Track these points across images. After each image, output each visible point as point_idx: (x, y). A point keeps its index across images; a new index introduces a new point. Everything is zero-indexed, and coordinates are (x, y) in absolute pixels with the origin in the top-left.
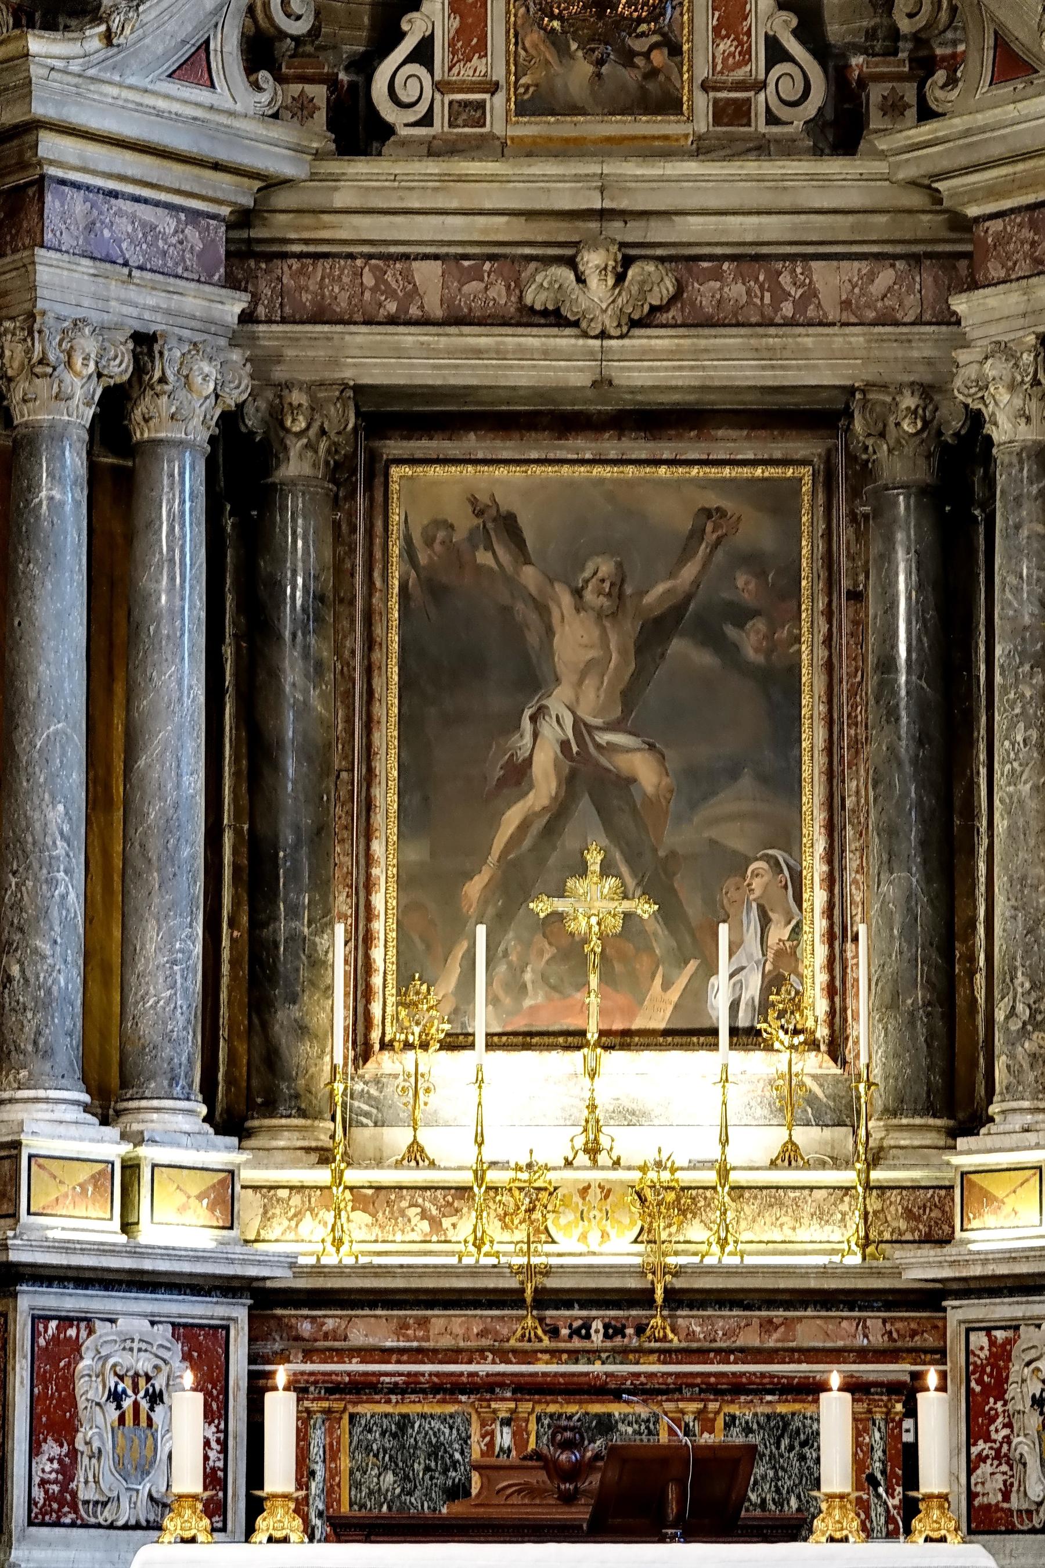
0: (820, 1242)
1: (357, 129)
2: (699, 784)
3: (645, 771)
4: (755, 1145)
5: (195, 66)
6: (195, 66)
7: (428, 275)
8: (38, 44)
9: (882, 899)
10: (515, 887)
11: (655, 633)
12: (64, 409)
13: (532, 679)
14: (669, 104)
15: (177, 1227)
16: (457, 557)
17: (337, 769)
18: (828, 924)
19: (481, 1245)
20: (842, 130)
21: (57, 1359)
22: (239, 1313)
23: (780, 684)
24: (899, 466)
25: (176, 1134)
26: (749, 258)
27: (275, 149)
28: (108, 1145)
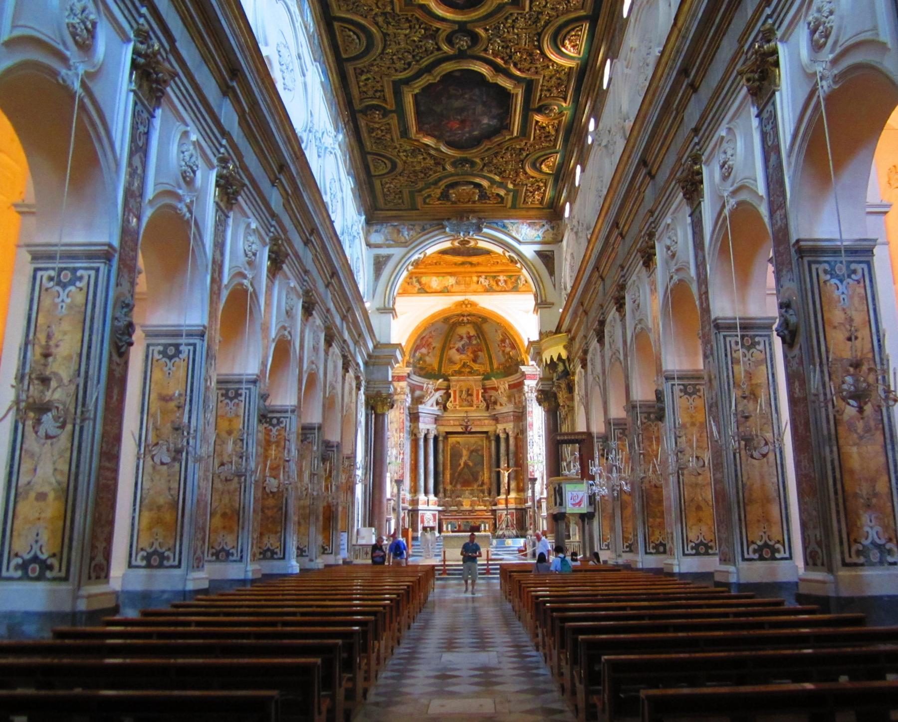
1: (445, 408)
3: (471, 464)
5: (432, 406)
6: (432, 406)
7: (452, 422)
8: (420, 406)
12: (422, 436)
13: (461, 456)
14: (472, 406)
16: (454, 446)
21: (422, 517)
22: (437, 513)
23: (483, 456)
24: (492, 438)
26: (479, 420)
28: (426, 498)
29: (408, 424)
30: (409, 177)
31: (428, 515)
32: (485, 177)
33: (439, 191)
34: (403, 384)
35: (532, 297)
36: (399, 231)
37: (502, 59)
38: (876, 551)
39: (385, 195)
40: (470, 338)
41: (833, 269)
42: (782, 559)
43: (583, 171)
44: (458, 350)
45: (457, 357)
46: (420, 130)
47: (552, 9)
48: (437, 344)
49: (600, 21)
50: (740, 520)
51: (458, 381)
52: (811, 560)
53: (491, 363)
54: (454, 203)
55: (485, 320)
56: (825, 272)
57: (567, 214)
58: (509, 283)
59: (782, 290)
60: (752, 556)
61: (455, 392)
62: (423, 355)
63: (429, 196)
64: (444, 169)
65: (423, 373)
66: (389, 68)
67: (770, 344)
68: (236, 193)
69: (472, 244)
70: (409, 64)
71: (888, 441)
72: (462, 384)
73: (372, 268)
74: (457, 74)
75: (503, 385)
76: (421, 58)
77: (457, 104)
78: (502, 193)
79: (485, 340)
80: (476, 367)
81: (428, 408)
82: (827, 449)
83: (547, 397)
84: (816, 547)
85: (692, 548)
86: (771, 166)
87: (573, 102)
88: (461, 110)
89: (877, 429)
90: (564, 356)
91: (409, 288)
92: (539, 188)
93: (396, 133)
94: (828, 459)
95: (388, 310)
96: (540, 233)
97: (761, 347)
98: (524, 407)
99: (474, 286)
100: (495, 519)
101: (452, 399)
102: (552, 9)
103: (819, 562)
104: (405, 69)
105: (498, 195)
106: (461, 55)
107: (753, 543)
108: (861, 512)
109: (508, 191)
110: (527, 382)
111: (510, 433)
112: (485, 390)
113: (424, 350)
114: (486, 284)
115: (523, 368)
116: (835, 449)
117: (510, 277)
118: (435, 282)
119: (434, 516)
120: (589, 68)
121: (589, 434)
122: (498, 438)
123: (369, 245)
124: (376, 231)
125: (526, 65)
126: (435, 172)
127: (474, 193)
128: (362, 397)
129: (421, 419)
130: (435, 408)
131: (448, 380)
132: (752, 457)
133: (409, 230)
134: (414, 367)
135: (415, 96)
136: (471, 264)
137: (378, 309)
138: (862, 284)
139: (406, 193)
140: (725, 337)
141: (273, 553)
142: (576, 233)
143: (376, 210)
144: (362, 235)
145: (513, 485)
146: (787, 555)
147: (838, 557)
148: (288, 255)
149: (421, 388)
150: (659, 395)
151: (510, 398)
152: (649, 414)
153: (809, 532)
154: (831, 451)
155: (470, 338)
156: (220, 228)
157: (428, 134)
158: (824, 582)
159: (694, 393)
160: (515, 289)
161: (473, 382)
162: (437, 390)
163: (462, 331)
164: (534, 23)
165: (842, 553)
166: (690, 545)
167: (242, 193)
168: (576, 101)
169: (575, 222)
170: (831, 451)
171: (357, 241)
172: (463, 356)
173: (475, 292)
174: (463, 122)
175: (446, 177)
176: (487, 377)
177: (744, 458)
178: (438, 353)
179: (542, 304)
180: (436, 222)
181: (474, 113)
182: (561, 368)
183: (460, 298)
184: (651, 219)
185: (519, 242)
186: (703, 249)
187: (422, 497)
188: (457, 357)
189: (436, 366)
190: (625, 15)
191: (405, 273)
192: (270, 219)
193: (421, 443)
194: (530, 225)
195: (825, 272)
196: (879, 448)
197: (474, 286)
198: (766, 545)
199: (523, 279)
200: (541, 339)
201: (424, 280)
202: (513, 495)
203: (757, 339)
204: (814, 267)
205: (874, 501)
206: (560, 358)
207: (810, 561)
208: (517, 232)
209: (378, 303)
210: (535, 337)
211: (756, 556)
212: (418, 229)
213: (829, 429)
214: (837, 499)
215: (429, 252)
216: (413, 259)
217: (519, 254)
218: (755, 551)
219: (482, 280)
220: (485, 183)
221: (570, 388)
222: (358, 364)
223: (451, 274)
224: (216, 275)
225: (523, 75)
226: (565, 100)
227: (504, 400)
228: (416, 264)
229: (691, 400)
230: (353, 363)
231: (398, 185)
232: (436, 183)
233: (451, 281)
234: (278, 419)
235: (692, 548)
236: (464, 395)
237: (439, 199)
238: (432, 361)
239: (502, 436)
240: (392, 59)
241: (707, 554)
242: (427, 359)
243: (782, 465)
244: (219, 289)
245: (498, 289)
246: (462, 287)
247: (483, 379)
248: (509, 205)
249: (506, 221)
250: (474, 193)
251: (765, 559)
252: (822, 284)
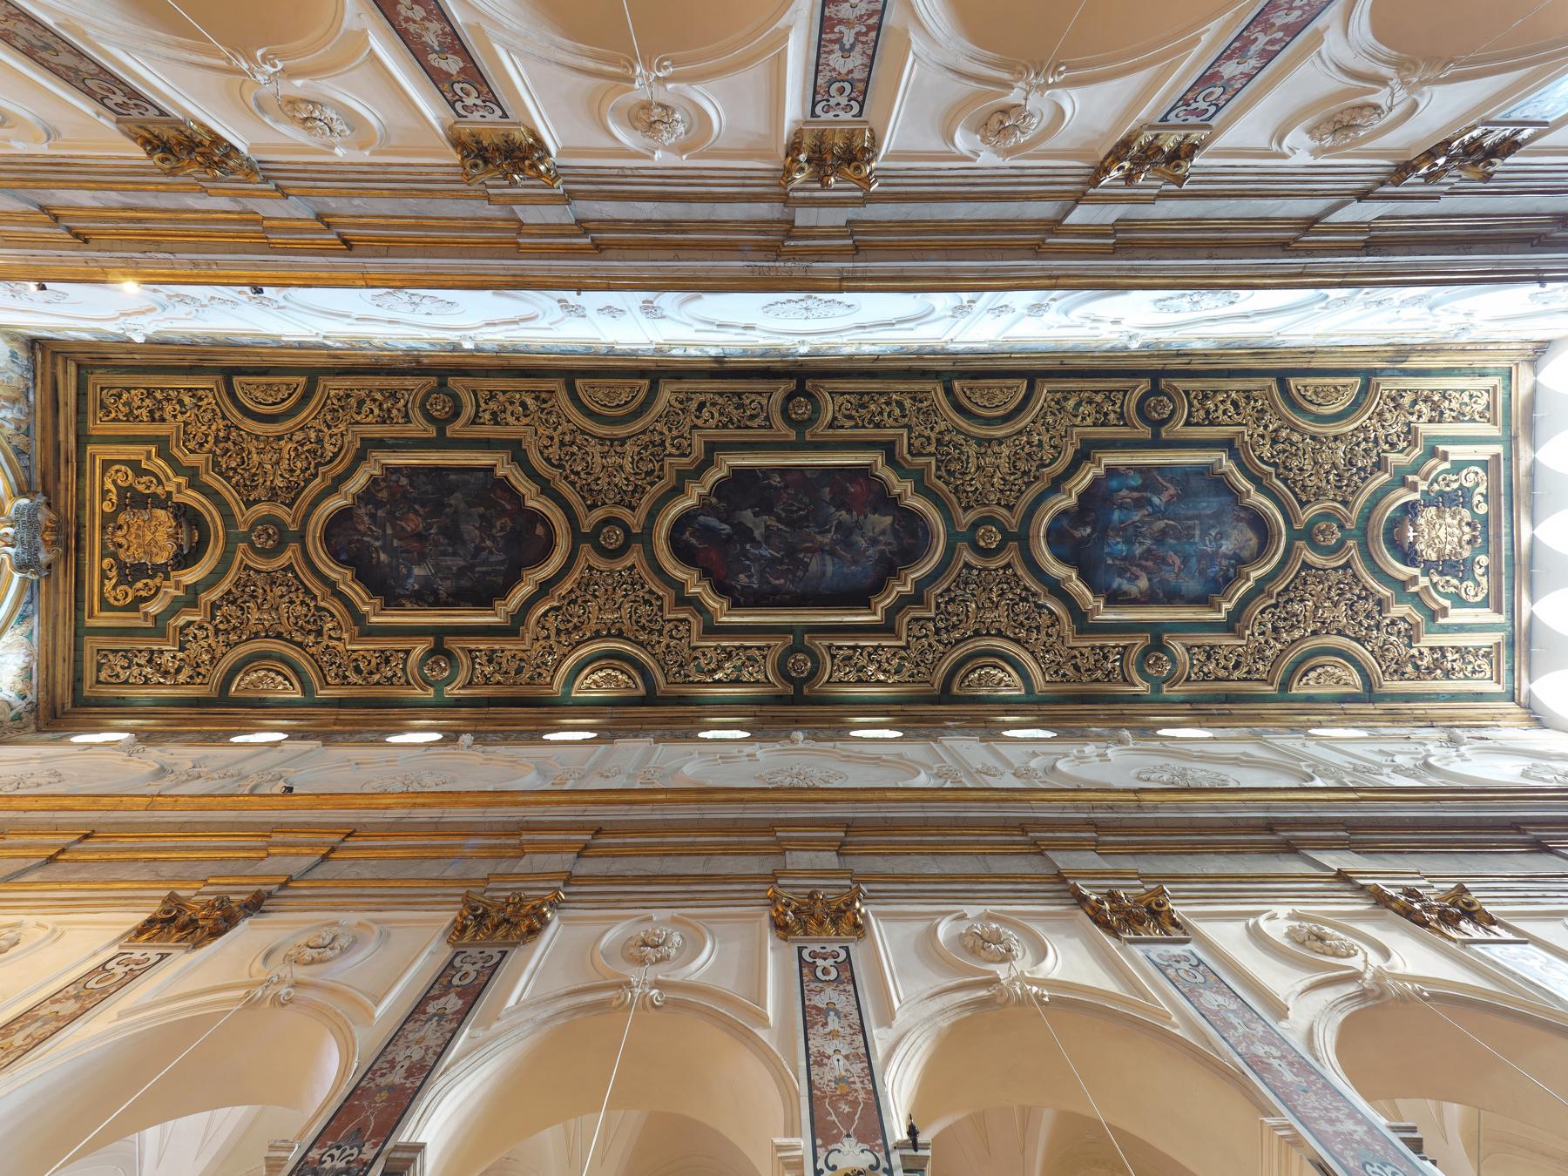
37: (572, 591)
46: (388, 469)
47: (668, 646)
49: (644, 709)
66: (552, 439)
70: (562, 467)
74: (540, 530)
76: (573, 484)
77: (470, 530)
87: (457, 700)
88: (453, 535)
93: (377, 431)
102: (668, 646)
104: (548, 460)
106: (577, 537)
120: (546, 709)
125: (552, 623)
135: (490, 470)
157: (374, 481)
164: (643, 628)
168: (459, 703)
174: (420, 537)
181: (444, 554)
190: (701, 735)
212: (19, 440)
225: (533, 620)
226: (470, 684)
240: (573, 443)
249: (36, 618)
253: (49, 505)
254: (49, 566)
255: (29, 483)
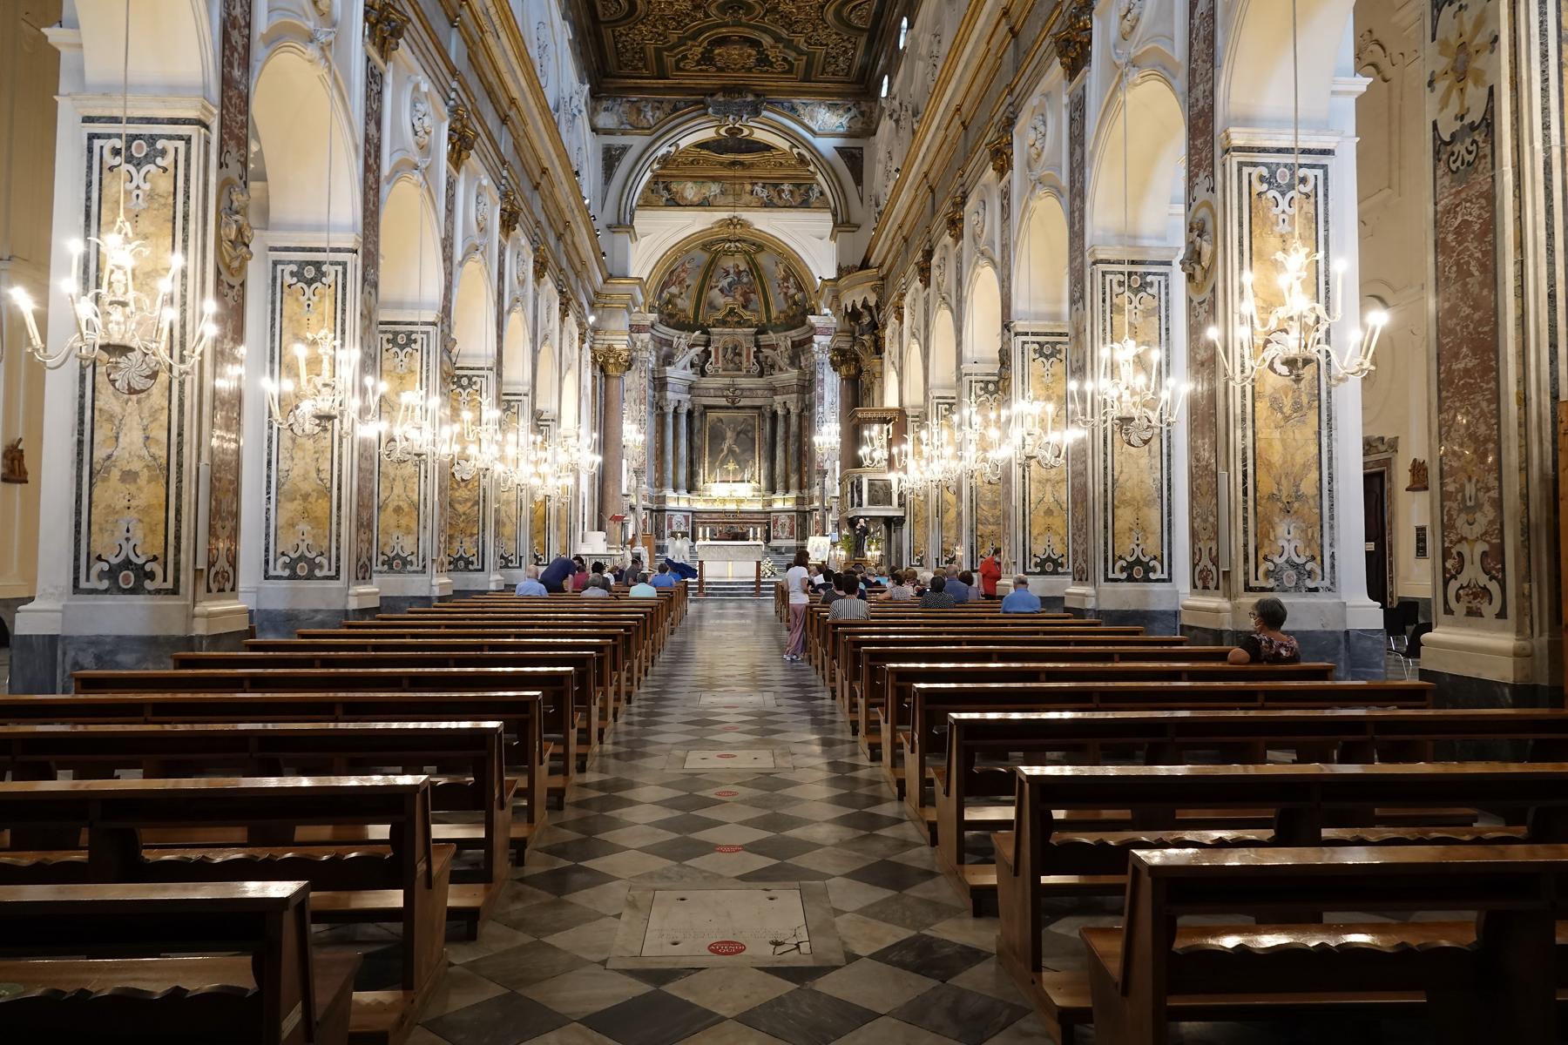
0: (758, 507)
1: (703, 373)
2: (744, 451)
4: (750, 494)
9: (765, 465)
10: (722, 463)
11: (738, 434)
15: (683, 505)
17: (702, 449)
18: (758, 469)
19: (718, 506)
20: (761, 374)
21: (670, 520)
24: (768, 415)
25: (683, 493)
27: (694, 378)
29: (651, 392)
30: (654, 26)
31: (678, 517)
32: (765, 31)
33: (700, 50)
34: (646, 336)
35: (829, 216)
36: (639, 111)
38: (1292, 572)
39: (618, 53)
40: (739, 273)
41: (1273, 174)
42: (1157, 581)
43: (911, 26)
44: (721, 290)
45: (720, 300)
48: (693, 281)
50: (1106, 527)
51: (721, 334)
52: (1202, 581)
53: (768, 310)
54: (720, 70)
55: (760, 248)
56: (1262, 179)
57: (884, 93)
58: (797, 194)
59: (1194, 205)
60: (1118, 575)
61: (717, 349)
62: (673, 296)
63: (685, 57)
64: (707, 15)
65: (672, 321)
67: (1167, 287)
68: (397, 33)
69: (746, 132)
71: (1324, 425)
72: (727, 338)
73: (600, 163)
75: (784, 340)
78: (792, 55)
79: (760, 277)
80: (747, 315)
81: (678, 373)
82: (1239, 433)
83: (842, 358)
84: (1210, 566)
85: (1036, 565)
86: (1197, 15)
89: (1310, 408)
90: (872, 303)
91: (653, 197)
92: (845, 52)
94: (1239, 447)
95: (623, 225)
96: (844, 120)
97: (1154, 291)
98: (813, 373)
99: (747, 198)
100: (768, 524)
101: (712, 359)
103: (1212, 584)
105: (785, 59)
107: (1120, 558)
108: (1277, 520)
109: (800, 53)
110: (817, 338)
111: (792, 409)
112: (758, 346)
113: (674, 290)
114: (764, 195)
115: (812, 319)
116: (1249, 433)
117: (798, 186)
118: (690, 191)
119: (686, 518)
121: (901, 412)
122: (775, 414)
123: (594, 129)
124: (606, 109)
126: (694, 19)
127: (750, 56)
128: (588, 356)
129: (669, 387)
130: (690, 371)
131: (708, 333)
132: (1129, 443)
133: (653, 108)
134: (661, 312)
136: (742, 163)
137: (609, 227)
138: (1312, 200)
139: (650, 48)
140: (1104, 274)
141: (468, 563)
142: (897, 121)
143: (606, 76)
144: (584, 113)
145: (794, 479)
146: (1165, 576)
147: (1241, 578)
148: (477, 135)
149: (669, 344)
150: (1005, 358)
151: (794, 361)
152: (987, 383)
153: (1201, 545)
154: (1244, 436)
155: (739, 273)
156: (374, 87)
158: (1217, 611)
159: (1052, 355)
160: (805, 204)
161: (743, 334)
162: (691, 346)
163: (728, 263)
165: (1246, 573)
166: (1034, 560)
167: (406, 34)
169: (896, 103)
170: (1244, 436)
171: (578, 121)
172: (730, 300)
173: (748, 206)
175: (709, 28)
176: (762, 331)
177: (1117, 444)
178: (693, 292)
179: (844, 224)
180: (698, 101)
182: (866, 320)
183: (725, 215)
184: (1009, 100)
185: (814, 133)
186: (1082, 145)
187: (669, 493)
188: (720, 300)
189: (691, 313)
191: (648, 174)
192: (449, 78)
193: (670, 419)
194: (832, 107)
195: (1262, 179)
196: (1310, 432)
197: (747, 198)
198: (1138, 562)
199: (816, 189)
200: (839, 277)
201: (674, 187)
202: (793, 494)
203: (1149, 278)
204: (1246, 171)
205: (1296, 505)
206: (865, 305)
207: (1199, 584)
208: (811, 118)
209: (609, 216)
210: (831, 274)
211: (1125, 575)
212: (667, 108)
213: (1244, 406)
214: (1245, 502)
215: (684, 143)
216: (659, 154)
217: (813, 150)
218: (1123, 569)
219: (758, 188)
220: (767, 40)
221: (879, 349)
222: (581, 305)
223: (714, 179)
224: (371, 161)
227: (783, 362)
228: (665, 161)
229: (1048, 365)
230: (574, 303)
231: (638, 38)
232: (694, 37)
233: (715, 188)
234: (470, 379)
235: (1036, 565)
236: (729, 355)
237: (698, 63)
238: (686, 304)
239: (780, 412)
241: (1055, 572)
242: (679, 301)
243: (1169, 455)
244: (378, 181)
245: (781, 203)
246: (731, 199)
247: (757, 333)
248: (801, 75)
249: (796, 101)
250: (750, 56)
251: (1136, 580)
252: (1254, 196)
253: (712, 95)
254: (757, 95)
255: (696, 103)
